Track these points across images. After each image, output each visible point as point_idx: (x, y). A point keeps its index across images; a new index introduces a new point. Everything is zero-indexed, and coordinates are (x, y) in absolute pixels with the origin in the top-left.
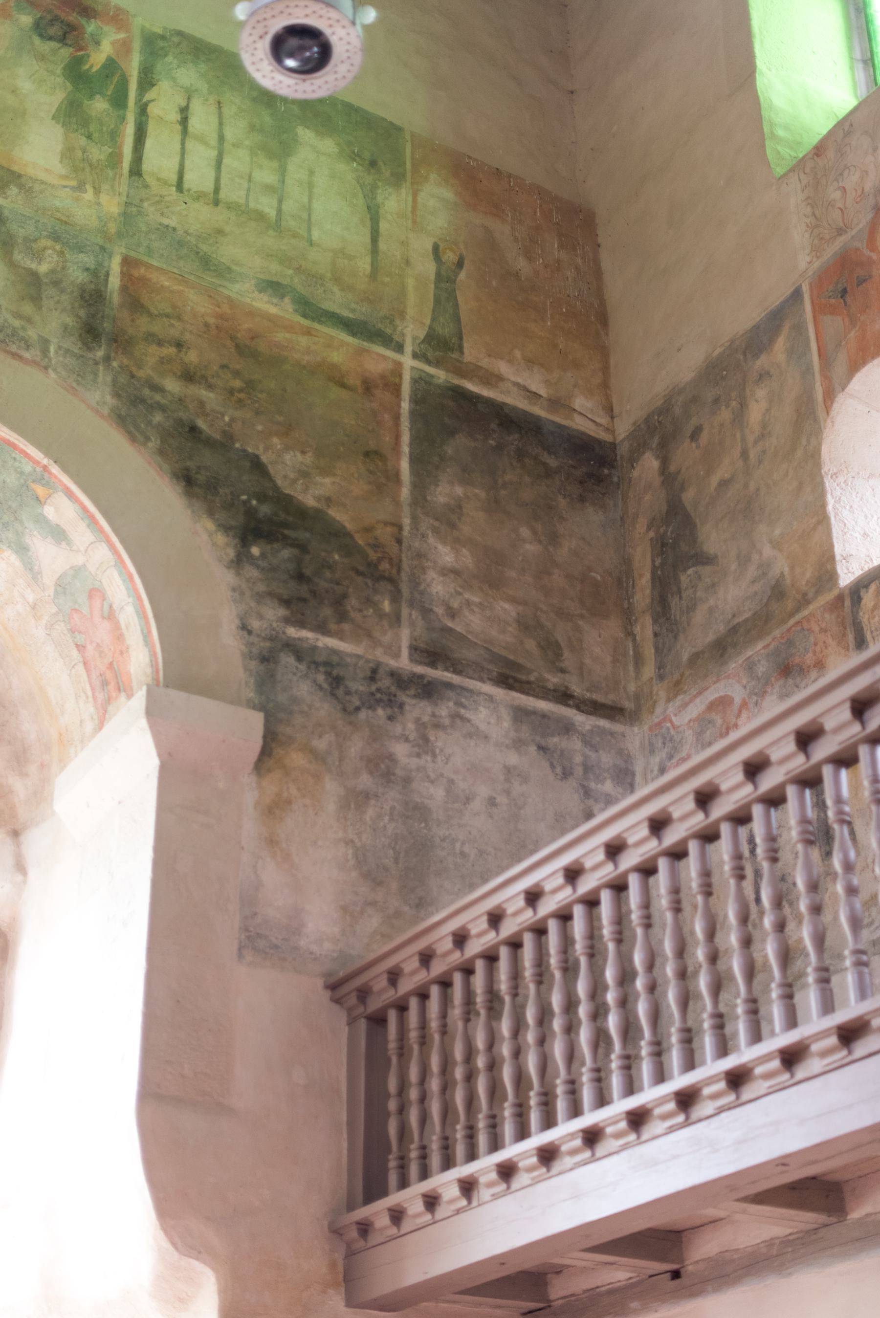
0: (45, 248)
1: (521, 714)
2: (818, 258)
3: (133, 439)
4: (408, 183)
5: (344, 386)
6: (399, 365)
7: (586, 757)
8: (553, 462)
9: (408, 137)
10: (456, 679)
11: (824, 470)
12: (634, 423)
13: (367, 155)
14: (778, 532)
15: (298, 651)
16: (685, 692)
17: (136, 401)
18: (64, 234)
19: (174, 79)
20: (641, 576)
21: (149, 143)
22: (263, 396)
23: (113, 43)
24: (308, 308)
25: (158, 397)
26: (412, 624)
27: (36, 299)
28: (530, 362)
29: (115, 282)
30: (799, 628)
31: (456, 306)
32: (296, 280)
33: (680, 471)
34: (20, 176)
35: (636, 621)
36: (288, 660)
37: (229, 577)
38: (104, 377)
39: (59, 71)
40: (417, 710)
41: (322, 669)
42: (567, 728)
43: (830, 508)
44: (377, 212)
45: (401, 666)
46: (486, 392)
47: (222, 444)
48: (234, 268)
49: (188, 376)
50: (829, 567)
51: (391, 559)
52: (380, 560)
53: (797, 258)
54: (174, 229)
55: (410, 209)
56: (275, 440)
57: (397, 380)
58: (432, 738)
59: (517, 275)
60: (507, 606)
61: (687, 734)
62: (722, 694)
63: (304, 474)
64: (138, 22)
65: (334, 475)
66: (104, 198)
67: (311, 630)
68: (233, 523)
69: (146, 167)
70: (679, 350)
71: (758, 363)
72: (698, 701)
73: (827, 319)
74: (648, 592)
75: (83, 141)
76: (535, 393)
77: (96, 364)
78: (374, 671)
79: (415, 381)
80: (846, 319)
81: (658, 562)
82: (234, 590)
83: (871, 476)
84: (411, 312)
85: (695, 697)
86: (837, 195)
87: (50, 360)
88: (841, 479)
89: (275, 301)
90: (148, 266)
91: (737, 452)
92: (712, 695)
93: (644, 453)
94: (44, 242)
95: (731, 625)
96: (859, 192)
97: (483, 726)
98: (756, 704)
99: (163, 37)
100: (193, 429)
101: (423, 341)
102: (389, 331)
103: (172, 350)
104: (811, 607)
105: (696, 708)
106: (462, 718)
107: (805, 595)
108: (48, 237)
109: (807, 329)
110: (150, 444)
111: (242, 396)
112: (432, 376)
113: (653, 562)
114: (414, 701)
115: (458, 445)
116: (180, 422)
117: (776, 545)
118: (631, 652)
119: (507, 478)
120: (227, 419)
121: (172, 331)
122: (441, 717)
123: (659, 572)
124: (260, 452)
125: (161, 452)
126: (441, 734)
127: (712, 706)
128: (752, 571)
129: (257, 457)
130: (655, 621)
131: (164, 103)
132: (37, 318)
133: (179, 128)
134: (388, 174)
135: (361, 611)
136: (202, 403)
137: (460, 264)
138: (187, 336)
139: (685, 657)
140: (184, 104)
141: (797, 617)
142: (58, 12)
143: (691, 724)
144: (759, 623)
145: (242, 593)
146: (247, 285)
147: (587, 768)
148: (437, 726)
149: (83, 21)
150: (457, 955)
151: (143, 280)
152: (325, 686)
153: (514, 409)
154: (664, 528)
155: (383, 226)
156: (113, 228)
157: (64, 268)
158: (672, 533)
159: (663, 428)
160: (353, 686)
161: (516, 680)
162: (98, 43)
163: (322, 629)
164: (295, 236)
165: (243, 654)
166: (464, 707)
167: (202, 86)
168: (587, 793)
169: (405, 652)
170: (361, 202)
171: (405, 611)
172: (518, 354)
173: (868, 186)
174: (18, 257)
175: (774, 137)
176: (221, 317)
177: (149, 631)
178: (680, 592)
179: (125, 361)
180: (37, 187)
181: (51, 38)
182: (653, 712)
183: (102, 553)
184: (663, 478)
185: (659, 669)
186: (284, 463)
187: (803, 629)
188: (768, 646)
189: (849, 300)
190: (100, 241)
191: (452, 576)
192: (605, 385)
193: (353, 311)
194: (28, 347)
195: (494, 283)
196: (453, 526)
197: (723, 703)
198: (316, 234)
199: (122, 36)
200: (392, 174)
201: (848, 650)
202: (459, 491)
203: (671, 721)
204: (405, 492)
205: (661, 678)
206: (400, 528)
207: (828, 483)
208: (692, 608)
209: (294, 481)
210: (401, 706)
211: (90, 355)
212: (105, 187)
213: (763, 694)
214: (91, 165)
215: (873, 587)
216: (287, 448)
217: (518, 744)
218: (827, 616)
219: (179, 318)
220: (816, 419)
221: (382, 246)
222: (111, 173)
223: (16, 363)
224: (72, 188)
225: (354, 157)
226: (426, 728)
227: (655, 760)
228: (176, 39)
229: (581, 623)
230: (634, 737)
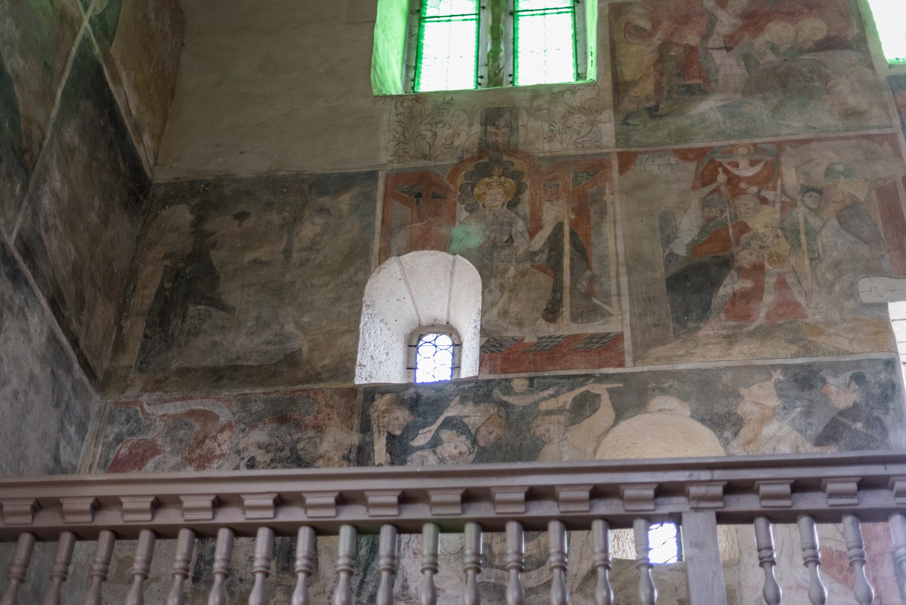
1: (52, 338)
2: (399, 162)
7: (70, 398)
8: (122, 168)
10: (31, 280)
11: (364, 299)
12: (177, 179)
14: (306, 319)
16: (167, 392)
20: (145, 287)
30: (305, 394)
31: (120, 9)
33: (214, 233)
35: (127, 318)
42: (69, 370)
43: (361, 325)
46: (110, 84)
50: (349, 365)
53: (383, 153)
60: (72, 248)
61: (157, 423)
62: (207, 408)
70: (241, 153)
71: (321, 200)
72: (178, 403)
73: (397, 204)
74: (148, 302)
80: (415, 213)
81: (167, 285)
83: (382, 321)
85: (177, 400)
86: (429, 134)
88: (370, 311)
91: (282, 246)
92: (196, 405)
93: (179, 203)
95: (233, 363)
96: (449, 142)
97: (32, 331)
98: (243, 430)
101: (97, 16)
104: (322, 385)
105: (174, 408)
106: (24, 313)
107: (318, 374)
109: (375, 201)
113: (162, 283)
117: (300, 327)
118: (114, 338)
123: (167, 293)
127: (191, 413)
128: (268, 335)
130: (149, 326)
139: (174, 366)
141: (305, 386)
143: (166, 418)
144: (265, 374)
147: (67, 408)
148: (10, 309)
150: (88, 518)
154: (183, 264)
158: (190, 272)
159: (207, 196)
161: (58, 309)
166: (28, 307)
168: (62, 428)
171: (25, 203)
173: (457, 143)
175: (375, 69)
178: (184, 317)
182: (123, 392)
184: (194, 230)
185: (141, 363)
187: (309, 397)
188: (268, 393)
189: (421, 202)
192: (159, 138)
197: (208, 417)
201: (352, 429)
203: (142, 407)
204: (54, 112)
205: (141, 370)
207: (364, 309)
208: (196, 333)
213: (253, 426)
215: (388, 397)
217: (43, 360)
218: (336, 398)
220: (368, 262)
227: (113, 431)
229: (98, 294)
230: (96, 402)
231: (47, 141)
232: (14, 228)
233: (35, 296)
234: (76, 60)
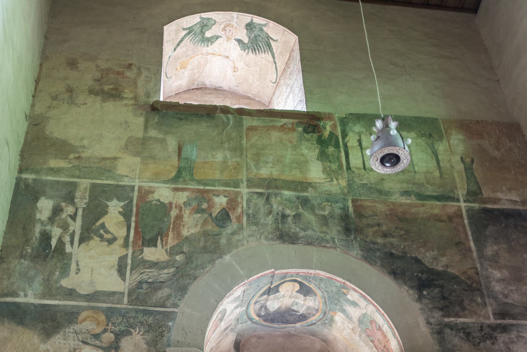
0: (325, 206)
3: (371, 264)
4: (445, 138)
5: (441, 221)
6: (460, 207)
9: (440, 121)
10: (514, 322)
13: (427, 133)
15: (451, 326)
17: (369, 250)
18: (330, 198)
19: (353, 131)
21: (350, 156)
22: (413, 234)
23: (330, 126)
24: (421, 197)
25: (376, 246)
26: (491, 305)
27: (326, 225)
28: (510, 190)
29: (351, 209)
31: (475, 178)
32: (414, 188)
34: (311, 183)
36: (447, 331)
37: (418, 306)
38: (356, 245)
39: (315, 143)
40: (502, 338)
41: (461, 331)
44: (437, 153)
45: (491, 322)
46: (496, 207)
47: (403, 256)
48: (391, 191)
49: (385, 235)
51: (476, 282)
52: (472, 283)
54: (367, 184)
55: (448, 147)
56: (422, 249)
57: (460, 213)
58: (512, 348)
59: (496, 158)
63: (435, 259)
64: (336, 116)
65: (447, 256)
66: (340, 181)
67: (453, 317)
68: (414, 285)
69: (352, 165)
75: (329, 164)
76: (515, 201)
77: (352, 241)
78: (482, 327)
79: (467, 211)
82: (421, 310)
84: (459, 186)
87: (336, 244)
89: (408, 198)
90: (361, 200)
94: (324, 204)
99: (346, 118)
100: (391, 254)
102: (452, 195)
103: (377, 228)
108: (325, 201)
110: (378, 264)
111: (405, 236)
112: (473, 207)
114: (500, 335)
115: (491, 230)
116: (386, 253)
119: (513, 237)
120: (402, 247)
121: (375, 221)
122: (513, 338)
124: (417, 255)
125: (382, 266)
126: (514, 345)
129: (416, 257)
131: (352, 141)
132: (328, 231)
133: (359, 147)
134: (437, 137)
135: (470, 305)
136: (392, 244)
137: (472, 161)
138: (381, 221)
140: (359, 138)
142: (309, 123)
145: (424, 310)
146: (397, 196)
148: (512, 342)
149: (319, 123)
151: (361, 206)
152: (464, 337)
153: (509, 209)
155: (440, 157)
156: (346, 191)
157: (333, 210)
160: (475, 335)
162: (325, 128)
163: (457, 316)
164: (409, 172)
165: (431, 333)
167: (364, 130)
169: (491, 316)
170: (429, 151)
171: (487, 300)
172: (504, 188)
174: (317, 212)
176: (391, 210)
177: (395, 333)
179: (362, 237)
180: (317, 185)
181: (310, 132)
183: (371, 308)
186: (427, 257)
190: (343, 197)
191: (502, 282)
193: (437, 192)
194: (328, 243)
195: (487, 164)
196: (497, 262)
198: (416, 169)
199: (333, 122)
200: (438, 137)
202: (495, 248)
204: (475, 254)
206: (477, 269)
209: (432, 263)
210: (496, 338)
211: (349, 239)
212: (340, 177)
214: (333, 172)
216: (426, 251)
219: (377, 215)
221: (442, 164)
222: (340, 172)
223: (325, 249)
224: (329, 181)
225: (422, 136)
226: (508, 344)
228: (350, 117)
231: (479, 268)
232: (489, 315)
233: (522, 325)
234: (469, 223)
